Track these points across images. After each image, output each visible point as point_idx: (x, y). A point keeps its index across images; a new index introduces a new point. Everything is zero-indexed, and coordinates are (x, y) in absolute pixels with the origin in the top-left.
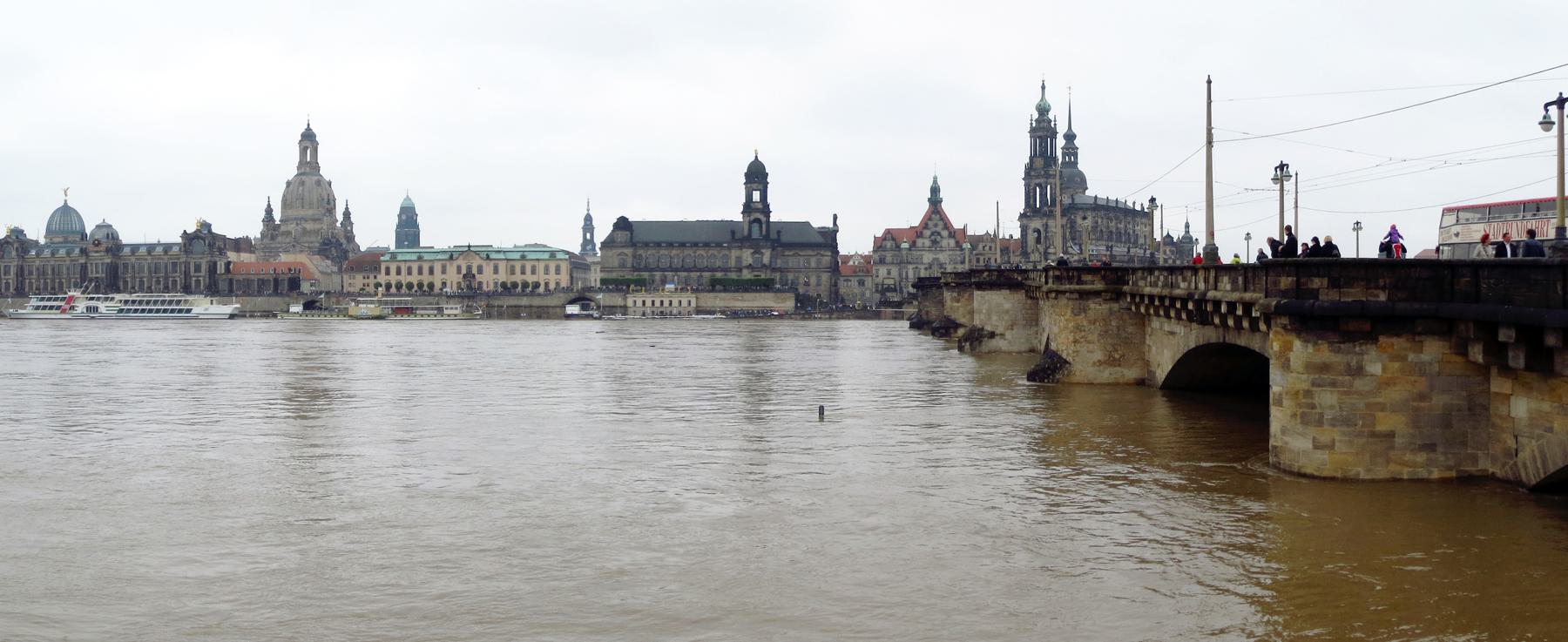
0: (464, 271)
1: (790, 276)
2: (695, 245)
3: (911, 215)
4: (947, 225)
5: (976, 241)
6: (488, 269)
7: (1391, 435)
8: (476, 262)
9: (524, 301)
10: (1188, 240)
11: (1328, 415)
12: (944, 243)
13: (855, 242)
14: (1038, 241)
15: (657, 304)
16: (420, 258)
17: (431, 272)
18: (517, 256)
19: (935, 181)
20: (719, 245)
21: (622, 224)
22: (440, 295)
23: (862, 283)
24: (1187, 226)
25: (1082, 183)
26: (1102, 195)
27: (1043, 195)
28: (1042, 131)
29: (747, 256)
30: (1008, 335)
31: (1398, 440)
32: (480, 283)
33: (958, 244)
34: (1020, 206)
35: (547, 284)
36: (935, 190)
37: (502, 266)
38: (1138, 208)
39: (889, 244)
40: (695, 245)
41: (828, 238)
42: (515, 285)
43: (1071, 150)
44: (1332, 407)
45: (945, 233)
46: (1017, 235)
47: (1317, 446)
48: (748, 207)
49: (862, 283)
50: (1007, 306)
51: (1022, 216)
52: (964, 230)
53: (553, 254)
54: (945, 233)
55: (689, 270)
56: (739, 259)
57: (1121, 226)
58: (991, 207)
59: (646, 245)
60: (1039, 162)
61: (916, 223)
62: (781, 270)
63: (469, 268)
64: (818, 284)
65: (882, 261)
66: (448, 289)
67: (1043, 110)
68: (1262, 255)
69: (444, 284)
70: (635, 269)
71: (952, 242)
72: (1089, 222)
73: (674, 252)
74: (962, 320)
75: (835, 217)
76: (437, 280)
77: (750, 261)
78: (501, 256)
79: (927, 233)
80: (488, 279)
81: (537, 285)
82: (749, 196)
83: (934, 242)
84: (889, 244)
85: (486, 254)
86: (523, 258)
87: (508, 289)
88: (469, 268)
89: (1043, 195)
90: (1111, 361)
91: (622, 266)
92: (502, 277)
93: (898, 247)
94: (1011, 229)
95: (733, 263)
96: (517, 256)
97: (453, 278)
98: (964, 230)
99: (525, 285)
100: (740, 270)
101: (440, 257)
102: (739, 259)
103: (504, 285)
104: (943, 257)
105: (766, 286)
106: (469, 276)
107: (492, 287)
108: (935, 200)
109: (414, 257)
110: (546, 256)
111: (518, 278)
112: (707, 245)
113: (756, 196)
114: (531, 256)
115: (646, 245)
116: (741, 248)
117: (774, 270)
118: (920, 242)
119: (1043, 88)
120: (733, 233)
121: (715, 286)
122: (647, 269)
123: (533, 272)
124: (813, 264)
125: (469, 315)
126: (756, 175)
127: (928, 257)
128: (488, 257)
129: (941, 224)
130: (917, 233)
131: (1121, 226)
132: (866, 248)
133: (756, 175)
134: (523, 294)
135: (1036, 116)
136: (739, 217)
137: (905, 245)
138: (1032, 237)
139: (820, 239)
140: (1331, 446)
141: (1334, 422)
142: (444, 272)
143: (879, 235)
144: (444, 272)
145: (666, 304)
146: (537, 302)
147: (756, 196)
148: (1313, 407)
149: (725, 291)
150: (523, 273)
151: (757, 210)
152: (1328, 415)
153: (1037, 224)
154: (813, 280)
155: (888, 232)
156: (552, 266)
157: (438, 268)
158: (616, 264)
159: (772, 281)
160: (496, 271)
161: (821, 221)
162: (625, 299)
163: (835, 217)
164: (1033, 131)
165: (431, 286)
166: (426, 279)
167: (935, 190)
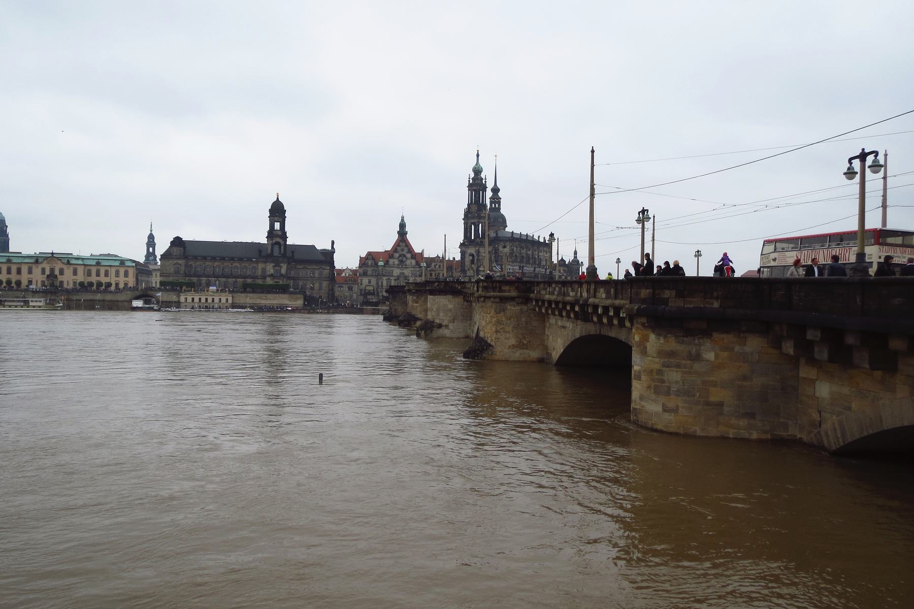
0: (48, 272)
1: (301, 283)
2: (232, 259)
3: (386, 242)
4: (410, 250)
5: (430, 261)
6: (68, 272)
7: (721, 404)
8: (58, 266)
9: (99, 297)
10: (576, 263)
11: (674, 388)
12: (408, 262)
13: (347, 260)
14: (472, 262)
15: (203, 300)
16: (9, 261)
17: (19, 271)
18: (94, 263)
19: (403, 220)
20: (250, 260)
21: (177, 242)
22: (26, 290)
23: (350, 289)
24: (575, 253)
25: (503, 222)
26: (517, 231)
27: (477, 231)
28: (477, 185)
29: (270, 268)
30: (451, 327)
31: (726, 409)
32: (62, 282)
33: (418, 264)
34: (461, 238)
35: (117, 284)
36: (402, 226)
37: (80, 270)
38: (542, 240)
40: (232, 259)
41: (328, 256)
42: (91, 284)
43: (496, 199)
44: (677, 382)
45: (409, 256)
46: (458, 258)
47: (666, 410)
48: (271, 234)
49: (350, 289)
50: (451, 306)
51: (462, 245)
52: (422, 254)
53: (122, 262)
54: (409, 256)
55: (227, 277)
56: (264, 270)
57: (530, 252)
58: (440, 236)
59: (195, 258)
60: (474, 208)
61: (389, 248)
62: (294, 279)
63: (52, 270)
64: (320, 289)
65: (365, 274)
66: (33, 287)
67: (477, 171)
68: (628, 273)
69: (30, 282)
70: (186, 275)
71: (413, 262)
72: (507, 250)
73: (216, 264)
74: (420, 316)
75: (333, 243)
76: (24, 278)
77: (272, 271)
78: (80, 262)
79: (397, 255)
80: (68, 279)
81: (109, 285)
82: (272, 226)
83: (401, 262)
85: (67, 260)
86: (98, 264)
87: (84, 287)
88: (52, 270)
89: (477, 231)
90: (520, 345)
91: (177, 272)
92: (80, 277)
93: (376, 264)
94: (454, 254)
95: (259, 272)
96: (94, 263)
97: (38, 277)
98: (422, 254)
99: (99, 284)
100: (264, 278)
101: (27, 260)
102: (264, 270)
103: (81, 284)
104: (407, 272)
105: (283, 290)
106: (52, 276)
107: (71, 286)
108: (402, 233)
109: (4, 260)
110: (117, 263)
111: (94, 279)
112: (241, 259)
113: (277, 226)
114: (104, 263)
115: (195, 258)
116: (265, 262)
117: (289, 278)
118: (391, 261)
119: (478, 155)
120: (260, 251)
121: (246, 288)
122: (195, 275)
123: (106, 275)
124: (317, 275)
125: (51, 306)
126: (277, 211)
127: (396, 272)
128: (68, 263)
129: (406, 249)
130: (388, 255)
131: (530, 252)
132: (354, 264)
133: (277, 211)
134: (98, 291)
135: (472, 175)
136: (264, 241)
137: (381, 263)
138: (468, 259)
139: (322, 258)
140: (675, 410)
141: (678, 393)
142: (30, 272)
143: (364, 255)
144: (30, 272)
145: (210, 300)
146: (109, 297)
147: (277, 226)
148: (663, 381)
149: (253, 292)
150: (98, 275)
151: (277, 236)
152: (674, 388)
153: (472, 250)
154: (317, 286)
155: (369, 254)
156: (122, 271)
157: (25, 269)
158: (172, 271)
159: (288, 286)
160: (75, 273)
161: (322, 245)
162: (179, 296)
163: (333, 243)
164: (470, 186)
165: (19, 283)
166: (14, 277)
167: (402, 226)
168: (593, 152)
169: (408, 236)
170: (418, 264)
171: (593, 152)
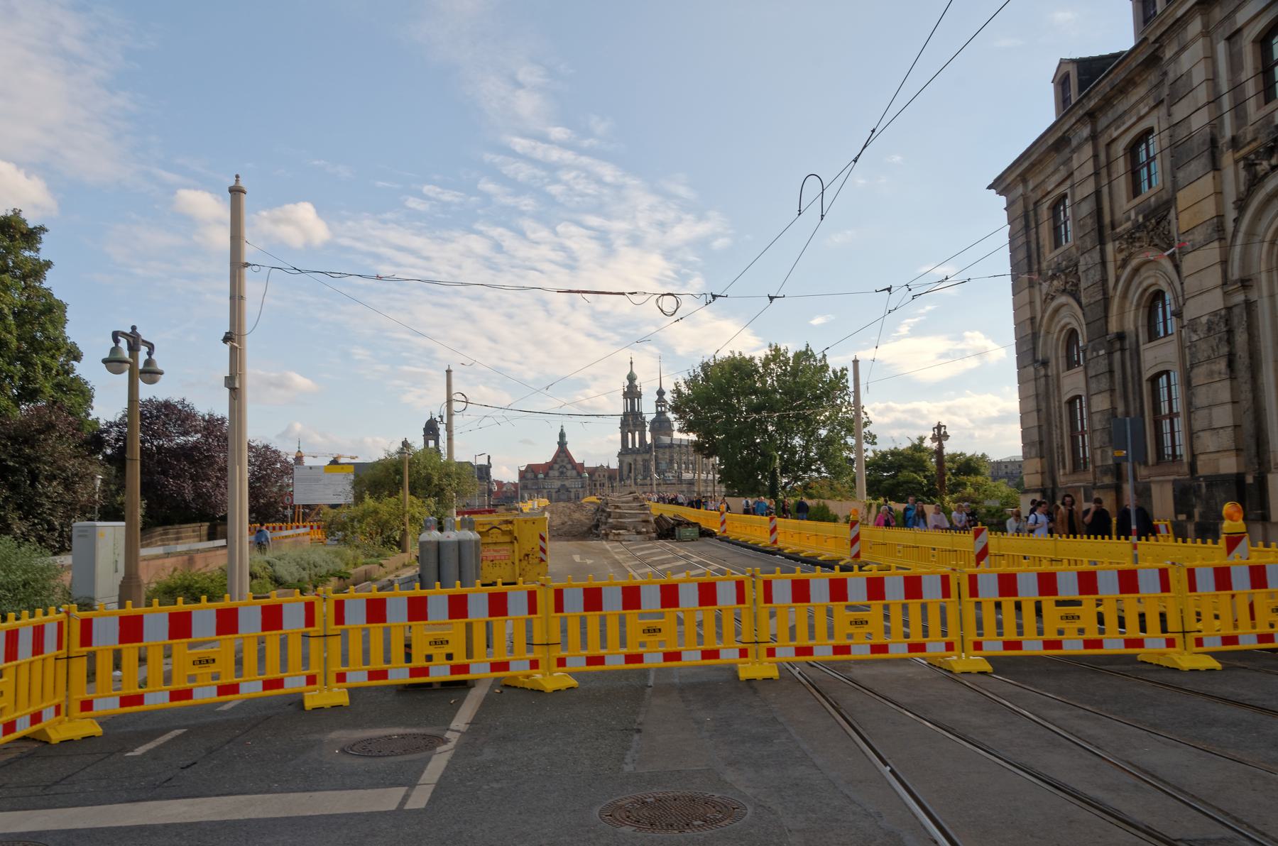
12: (569, 473)
36: (562, 435)
39: (529, 475)
45: (569, 466)
54: (569, 466)
65: (525, 487)
71: (574, 473)
83: (562, 473)
84: (529, 475)
93: (536, 477)
104: (567, 483)
118: (552, 473)
127: (557, 484)
130: (548, 467)
153: (629, 459)
167: (562, 435)
169: (569, 447)
170: (579, 474)
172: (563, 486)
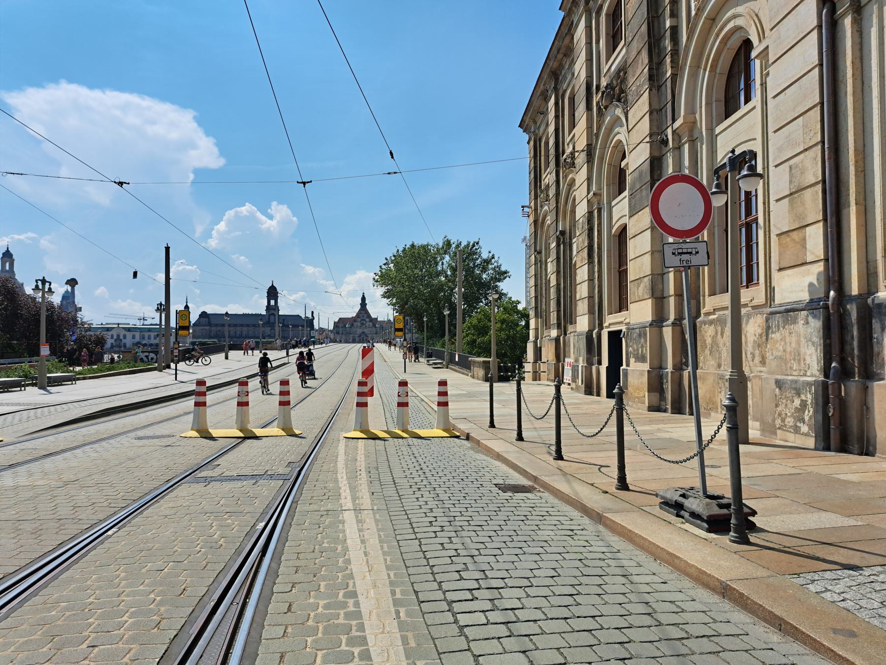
3: (352, 312)
4: (369, 316)
12: (367, 324)
45: (368, 320)
54: (368, 320)
71: (371, 324)
83: (362, 324)
84: (341, 325)
93: (345, 326)
104: (366, 331)
118: (355, 324)
127: (359, 331)
130: (354, 320)
143: (337, 320)
168: (167, 249)
169: (367, 307)
170: (374, 325)
171: (167, 249)
172: (363, 333)
